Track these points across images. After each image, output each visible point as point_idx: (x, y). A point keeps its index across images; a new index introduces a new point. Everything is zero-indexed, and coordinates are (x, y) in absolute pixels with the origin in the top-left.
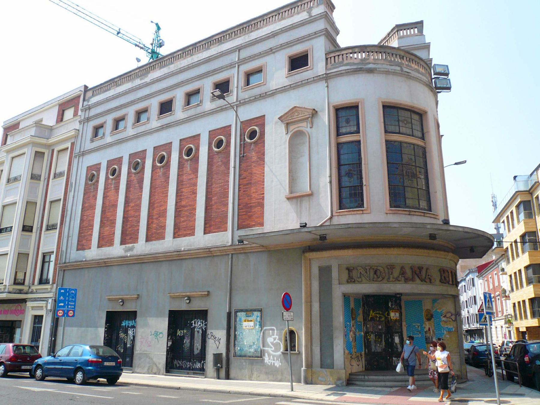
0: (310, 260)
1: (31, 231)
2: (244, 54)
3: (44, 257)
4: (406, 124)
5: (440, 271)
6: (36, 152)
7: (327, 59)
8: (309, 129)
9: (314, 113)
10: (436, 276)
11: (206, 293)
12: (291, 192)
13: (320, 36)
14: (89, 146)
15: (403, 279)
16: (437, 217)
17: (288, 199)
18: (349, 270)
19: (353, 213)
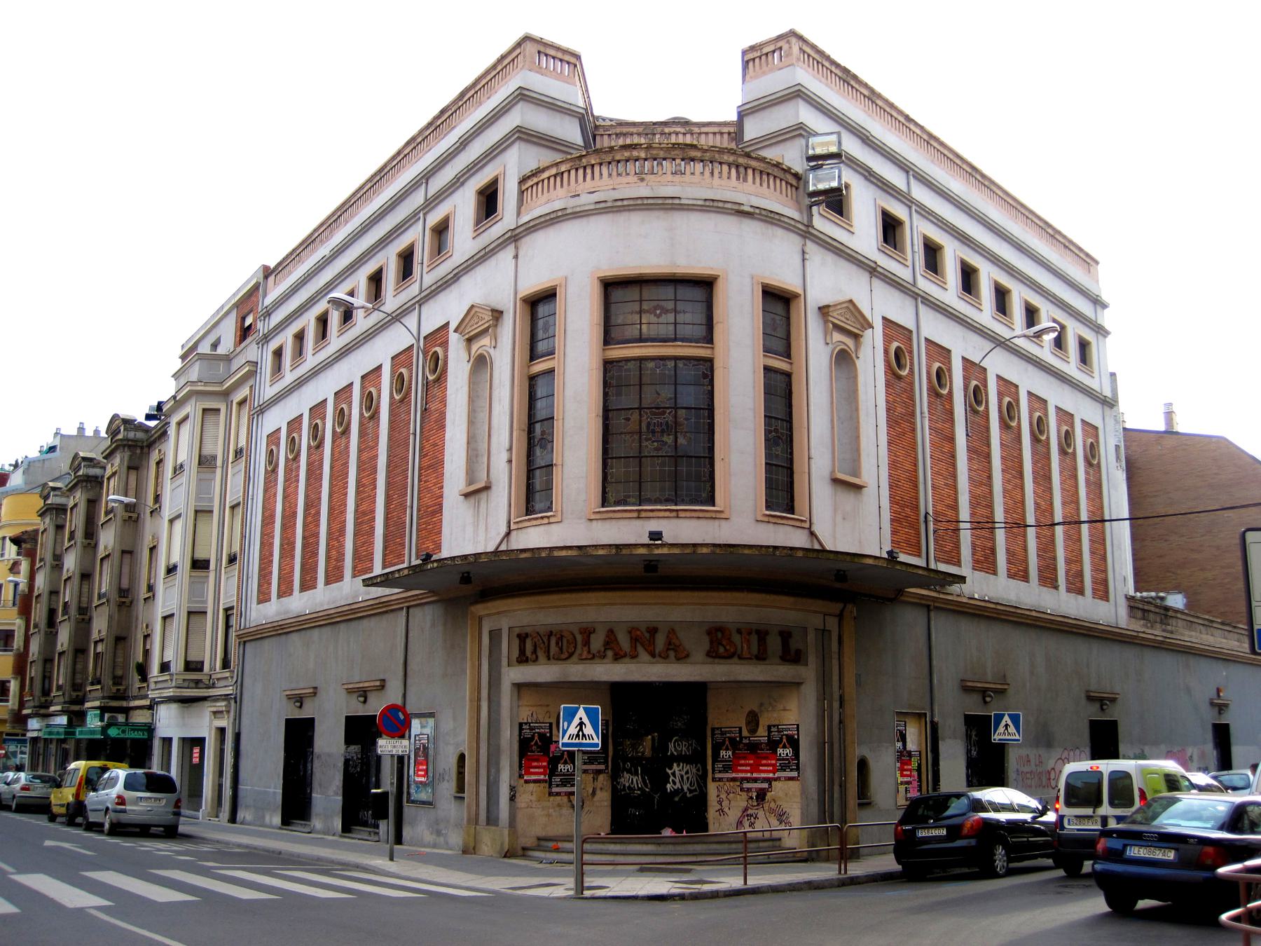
0: (480, 619)
1: (207, 568)
2: (437, 183)
3: (227, 618)
4: (659, 316)
5: (709, 633)
6: (204, 410)
7: (521, 193)
8: (492, 351)
9: (497, 314)
10: (697, 644)
11: (378, 683)
12: (470, 482)
13: (513, 143)
14: (269, 392)
15: (610, 653)
16: (718, 515)
17: (467, 495)
18: (522, 638)
19: (535, 523)
